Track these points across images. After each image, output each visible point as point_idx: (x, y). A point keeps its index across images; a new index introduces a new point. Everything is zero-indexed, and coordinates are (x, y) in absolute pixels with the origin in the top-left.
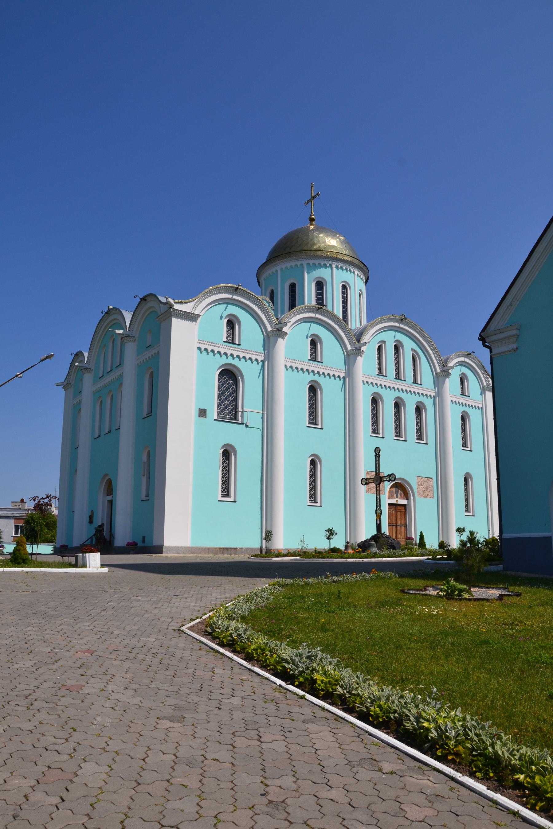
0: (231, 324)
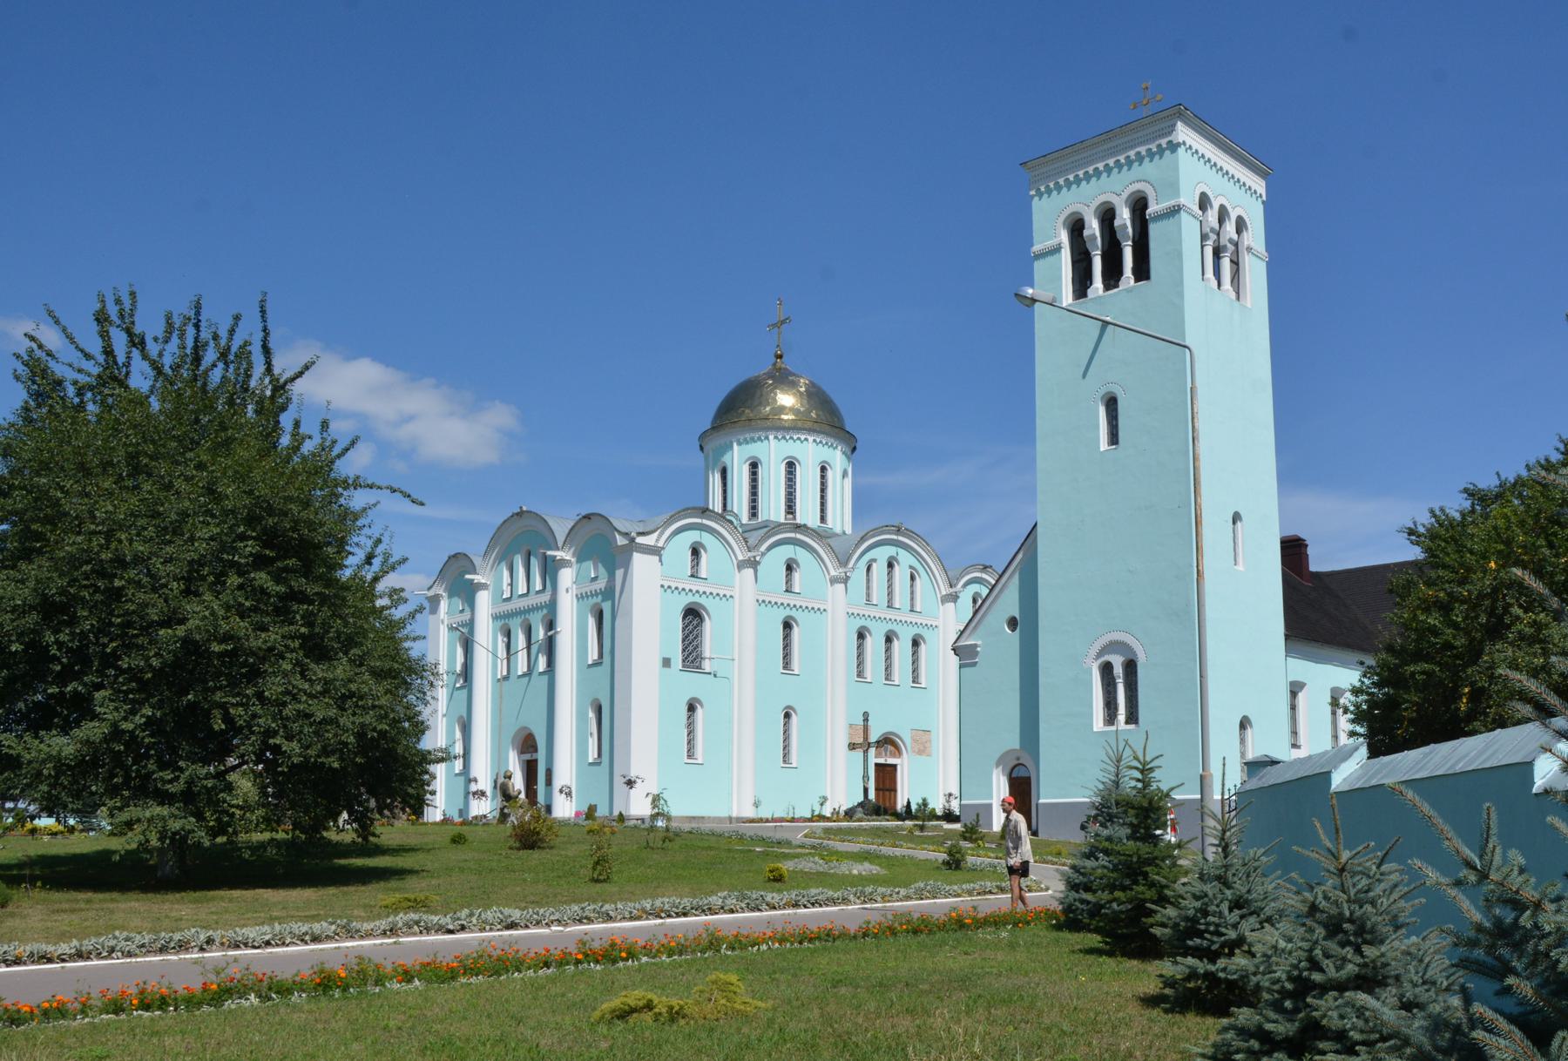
0: (695, 552)
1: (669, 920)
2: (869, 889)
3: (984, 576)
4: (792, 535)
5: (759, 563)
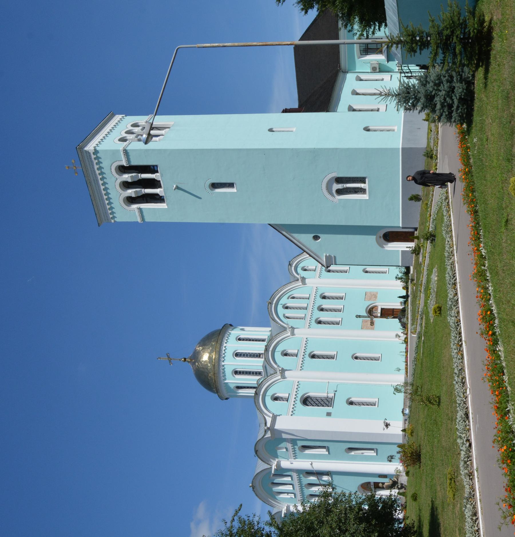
0: (276, 399)
1: (463, 339)
2: (446, 254)
3: (294, 265)
4: (270, 352)
5: (282, 369)
